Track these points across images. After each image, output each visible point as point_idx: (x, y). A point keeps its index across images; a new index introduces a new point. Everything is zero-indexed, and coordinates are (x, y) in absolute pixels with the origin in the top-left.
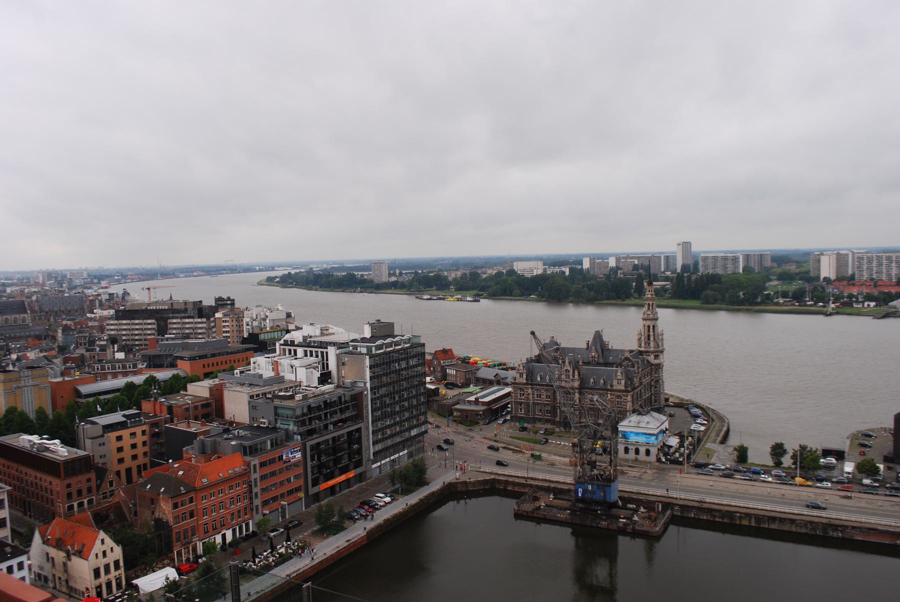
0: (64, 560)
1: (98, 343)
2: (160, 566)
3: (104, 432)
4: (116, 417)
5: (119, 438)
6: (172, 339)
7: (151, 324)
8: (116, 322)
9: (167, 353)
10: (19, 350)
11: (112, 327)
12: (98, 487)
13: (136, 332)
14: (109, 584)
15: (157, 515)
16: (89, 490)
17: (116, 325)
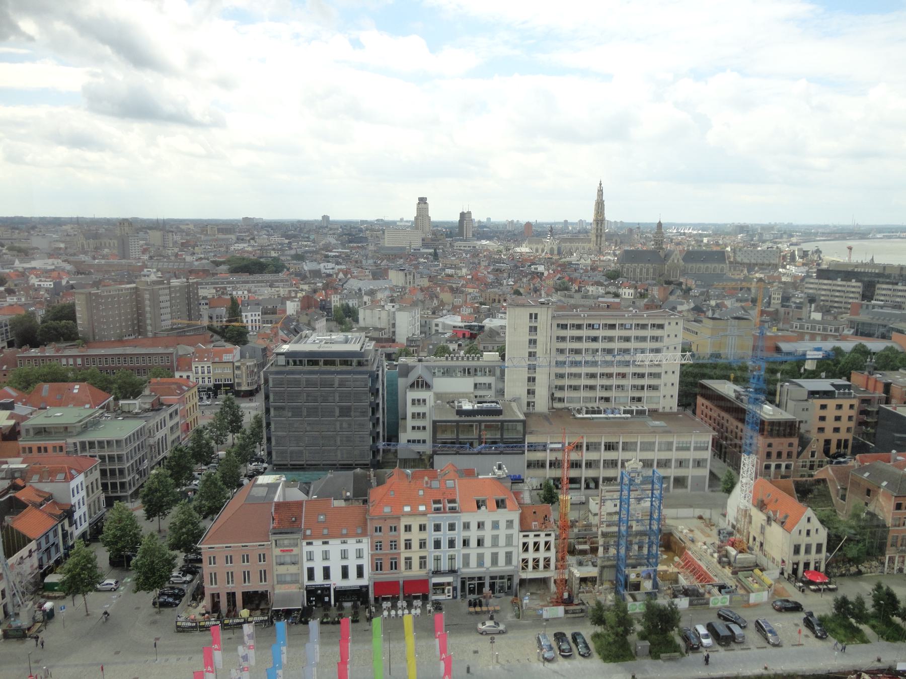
0: (764, 523)
1: (793, 299)
2: (867, 566)
3: (809, 397)
4: (824, 384)
5: (823, 407)
6: (882, 307)
7: (855, 286)
8: (817, 281)
9: (880, 322)
10: (718, 297)
11: (812, 286)
12: (799, 454)
13: (837, 294)
14: (807, 565)
15: (871, 508)
16: (789, 455)
17: (816, 284)
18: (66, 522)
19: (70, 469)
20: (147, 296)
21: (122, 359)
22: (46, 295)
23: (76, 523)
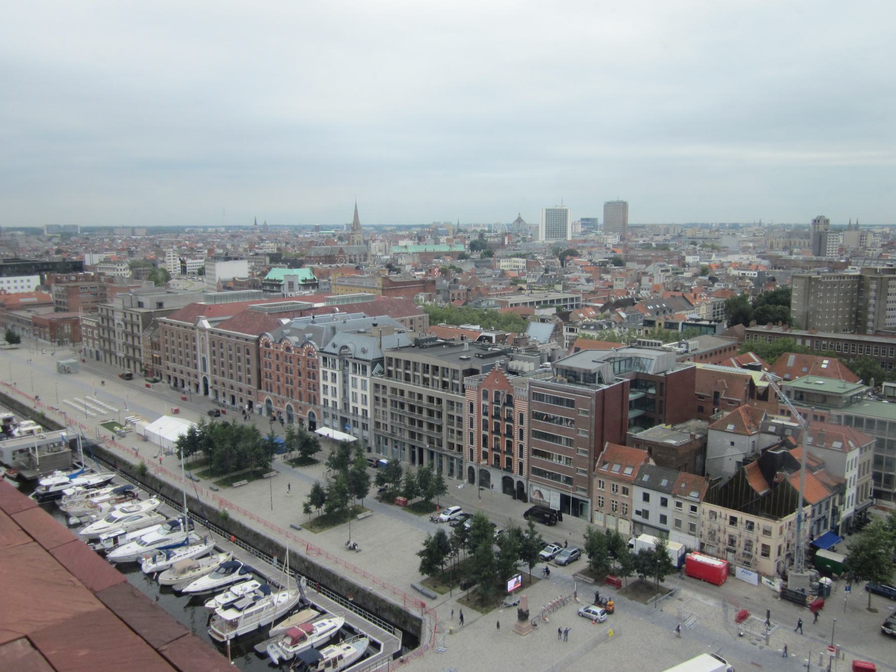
18: (837, 497)
19: (847, 439)
20: (873, 286)
21: (857, 347)
22: (752, 284)
23: (844, 503)
